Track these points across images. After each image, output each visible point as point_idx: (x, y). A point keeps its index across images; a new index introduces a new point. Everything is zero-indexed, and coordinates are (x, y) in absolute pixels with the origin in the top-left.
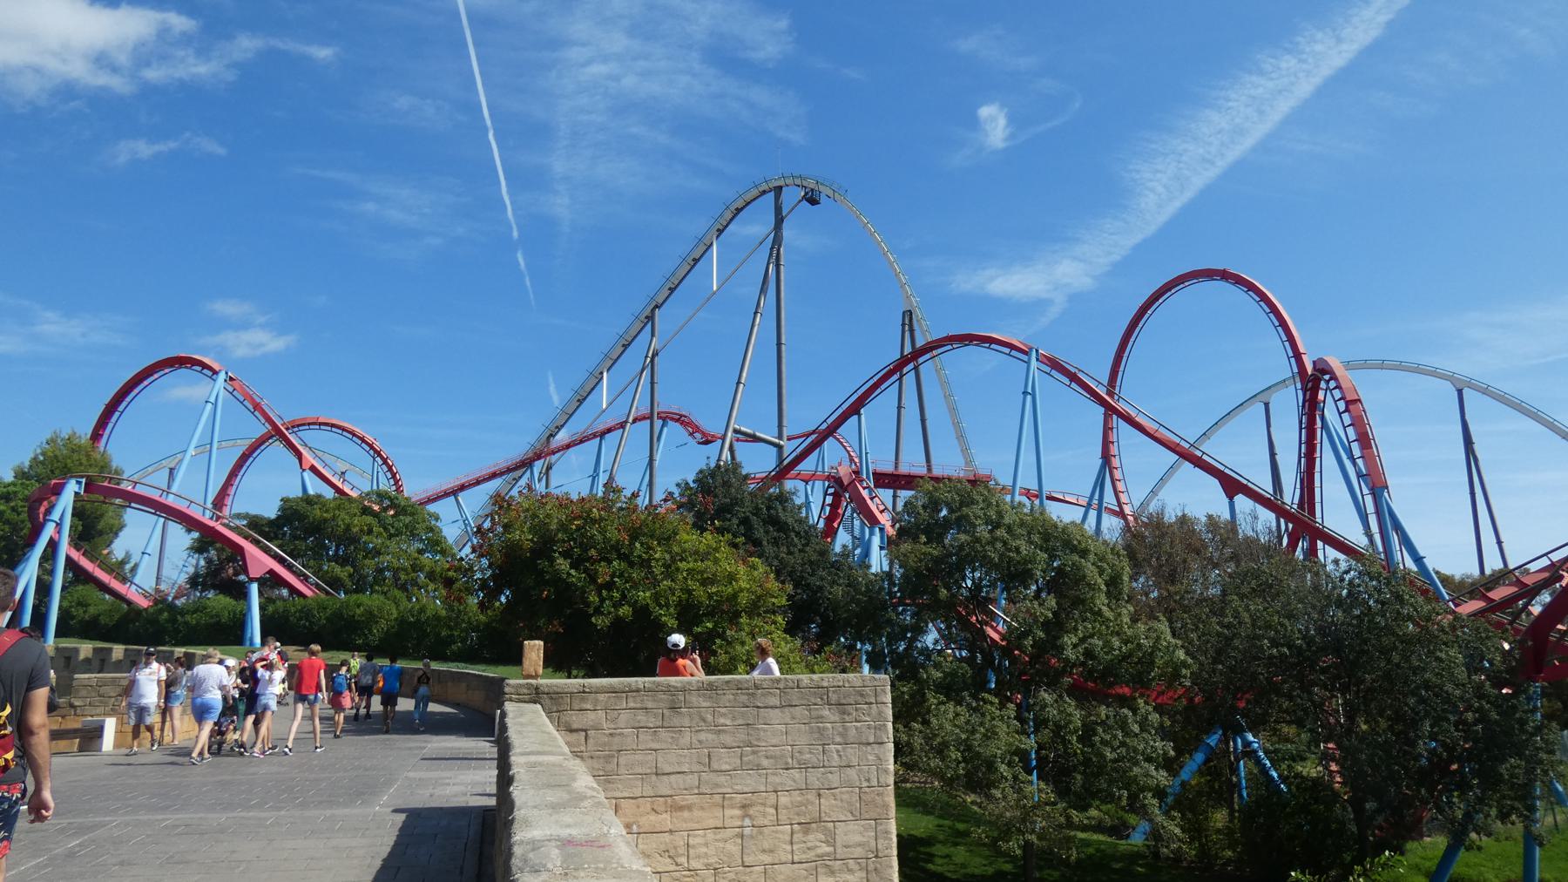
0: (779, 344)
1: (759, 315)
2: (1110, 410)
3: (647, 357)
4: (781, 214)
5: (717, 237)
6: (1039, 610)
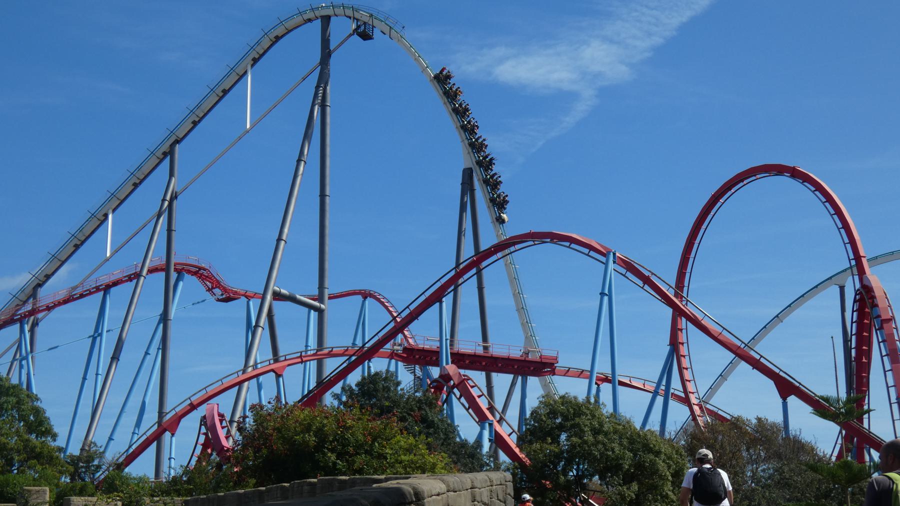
0: (323, 196)
1: (303, 163)
2: (678, 313)
3: (164, 200)
4: (329, 48)
5: (252, 66)
6: (627, 493)
